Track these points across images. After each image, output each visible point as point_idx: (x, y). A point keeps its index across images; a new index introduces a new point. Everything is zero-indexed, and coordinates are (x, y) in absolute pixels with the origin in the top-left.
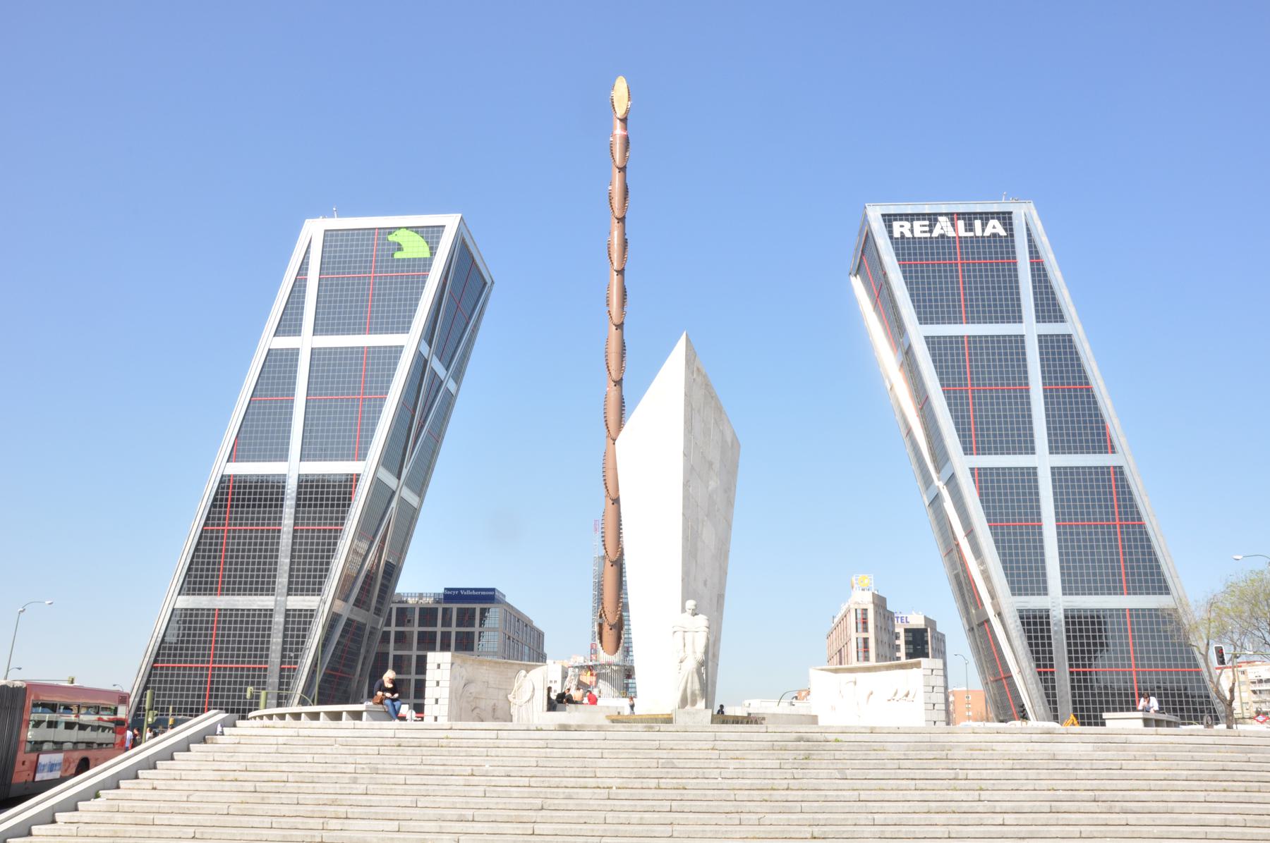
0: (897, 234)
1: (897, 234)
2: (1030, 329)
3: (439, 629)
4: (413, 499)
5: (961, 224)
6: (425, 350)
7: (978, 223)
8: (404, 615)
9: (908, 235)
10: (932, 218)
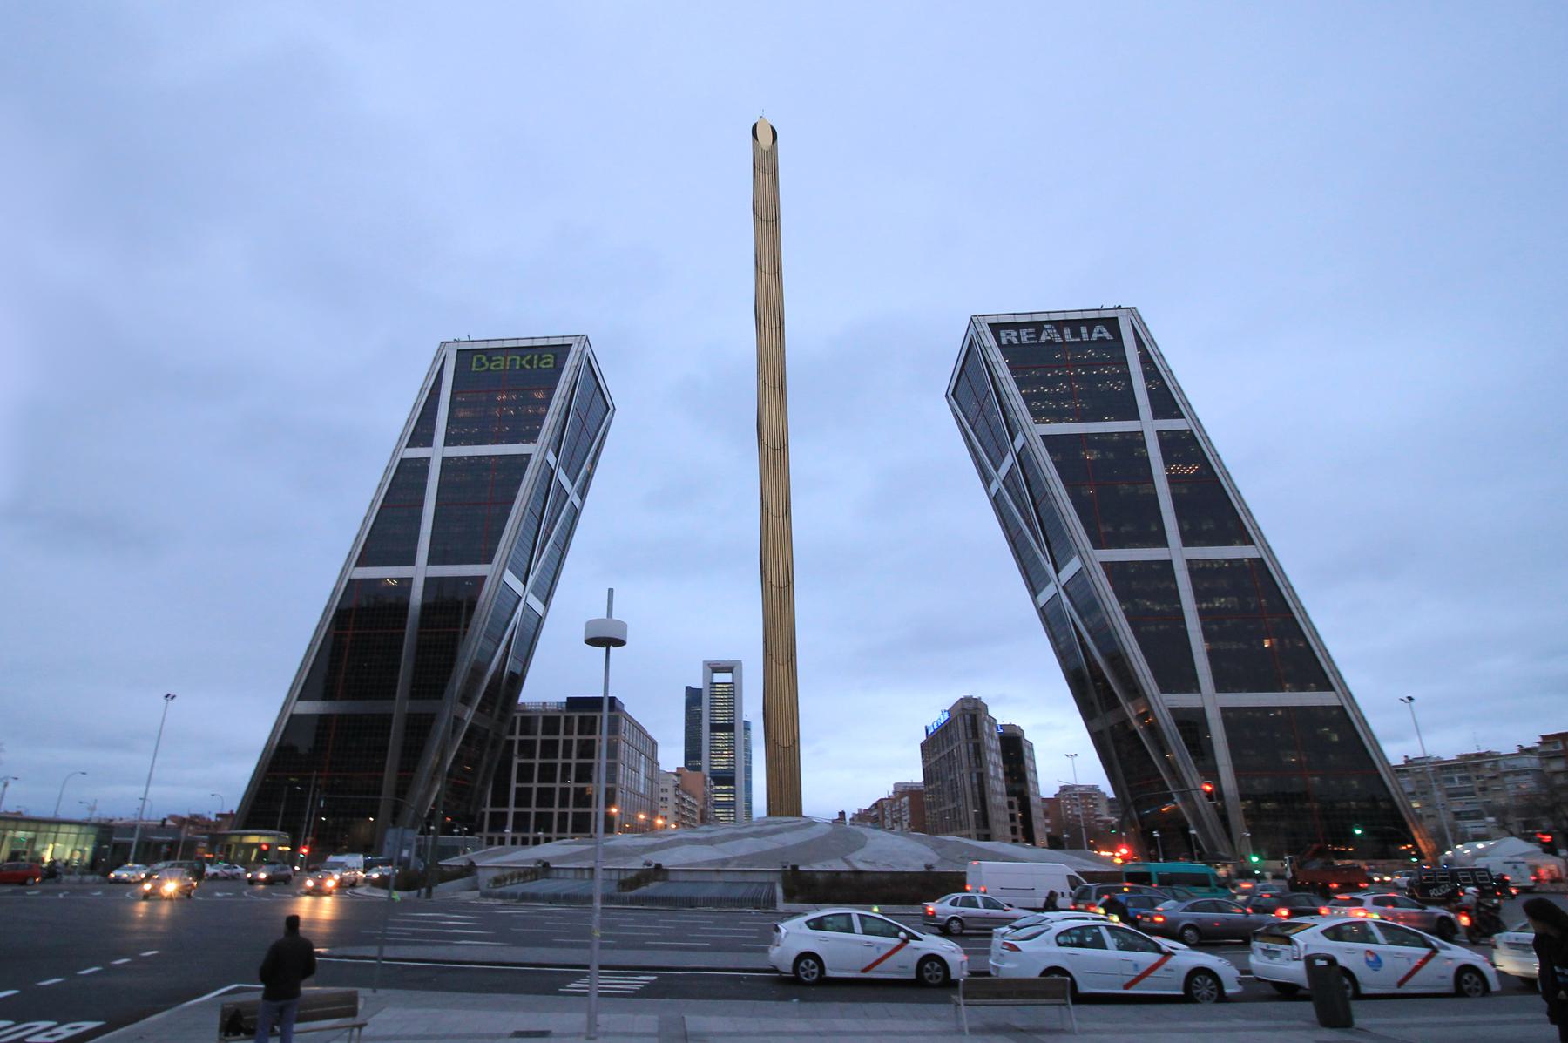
0: (1004, 341)
1: (1004, 341)
2: (1148, 426)
3: (575, 737)
4: (538, 607)
5: (1067, 331)
6: (551, 458)
7: (1084, 330)
8: (528, 723)
9: (1015, 341)
10: (1037, 326)
